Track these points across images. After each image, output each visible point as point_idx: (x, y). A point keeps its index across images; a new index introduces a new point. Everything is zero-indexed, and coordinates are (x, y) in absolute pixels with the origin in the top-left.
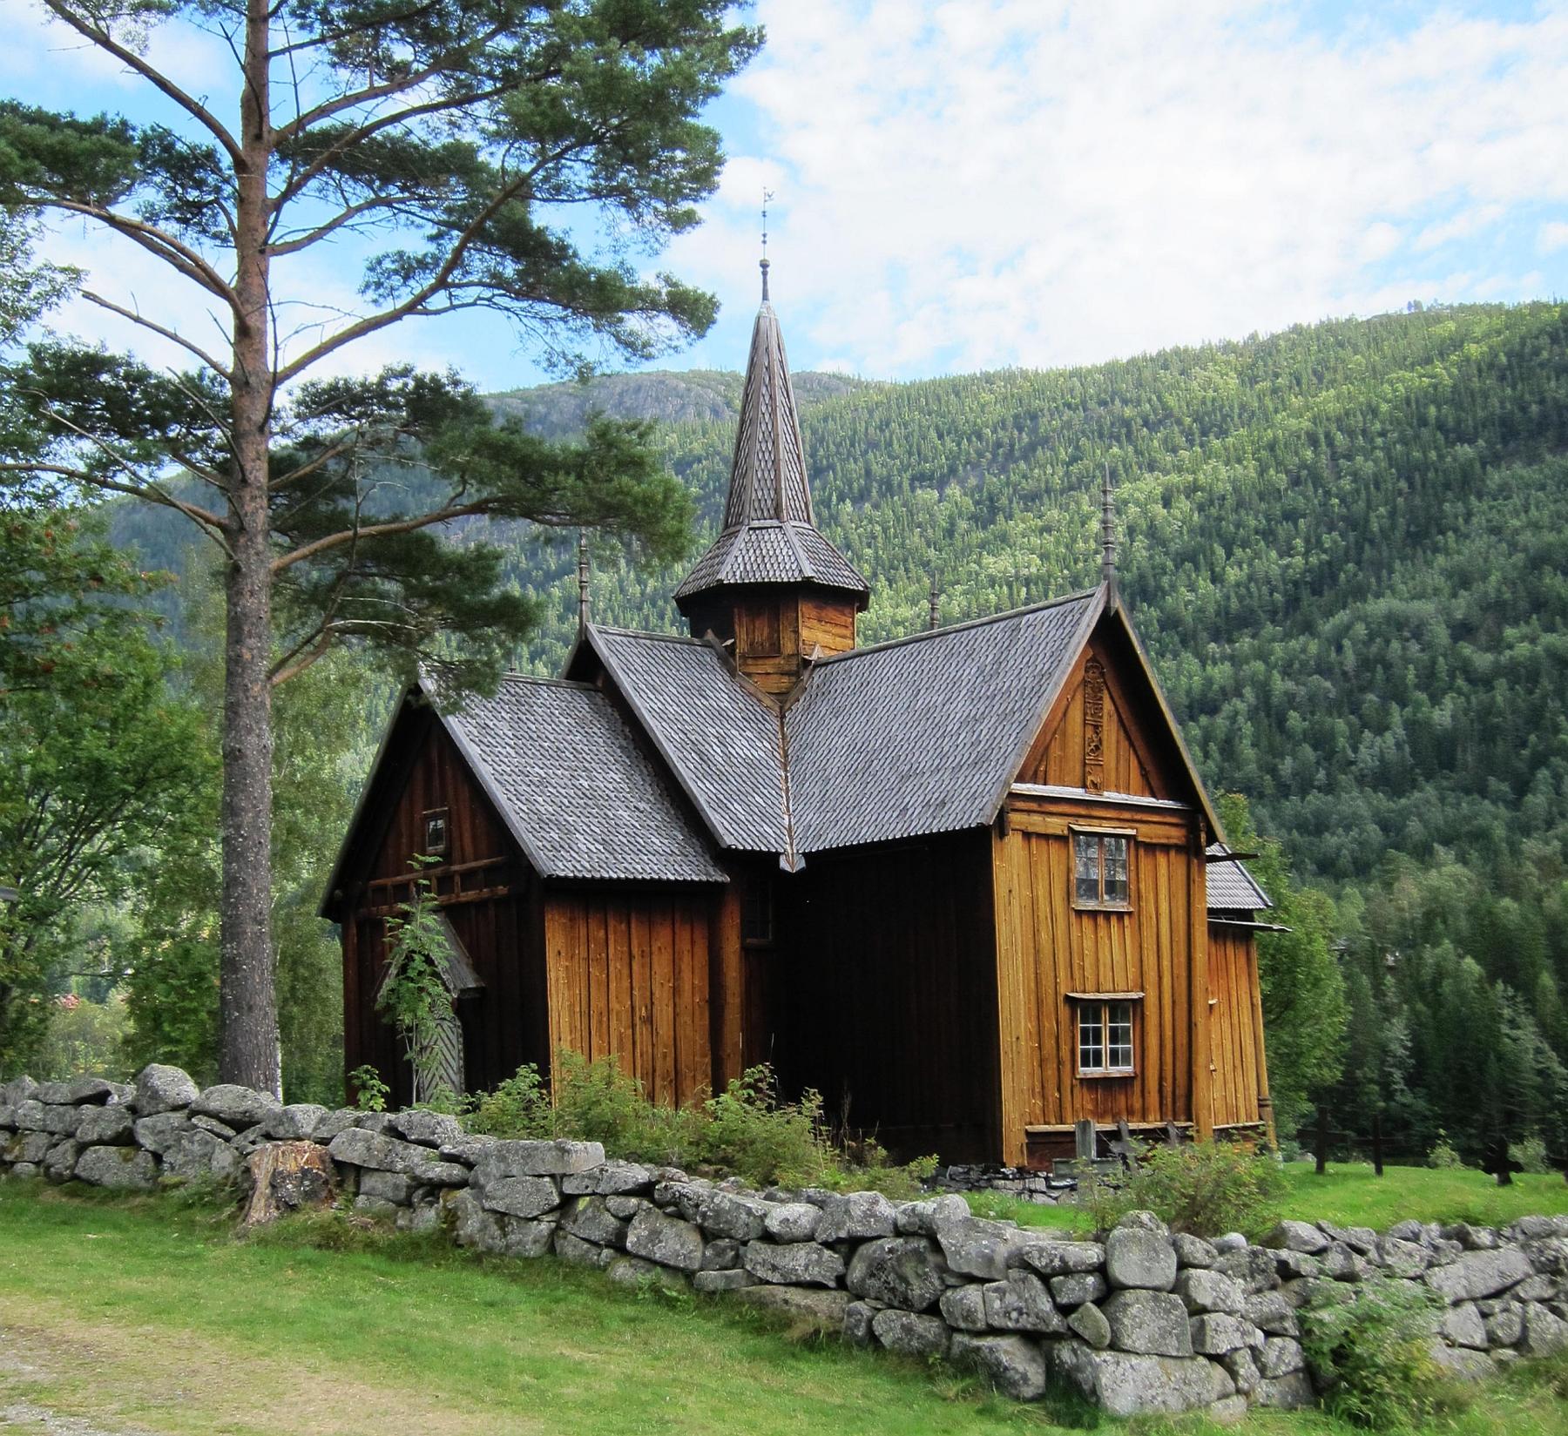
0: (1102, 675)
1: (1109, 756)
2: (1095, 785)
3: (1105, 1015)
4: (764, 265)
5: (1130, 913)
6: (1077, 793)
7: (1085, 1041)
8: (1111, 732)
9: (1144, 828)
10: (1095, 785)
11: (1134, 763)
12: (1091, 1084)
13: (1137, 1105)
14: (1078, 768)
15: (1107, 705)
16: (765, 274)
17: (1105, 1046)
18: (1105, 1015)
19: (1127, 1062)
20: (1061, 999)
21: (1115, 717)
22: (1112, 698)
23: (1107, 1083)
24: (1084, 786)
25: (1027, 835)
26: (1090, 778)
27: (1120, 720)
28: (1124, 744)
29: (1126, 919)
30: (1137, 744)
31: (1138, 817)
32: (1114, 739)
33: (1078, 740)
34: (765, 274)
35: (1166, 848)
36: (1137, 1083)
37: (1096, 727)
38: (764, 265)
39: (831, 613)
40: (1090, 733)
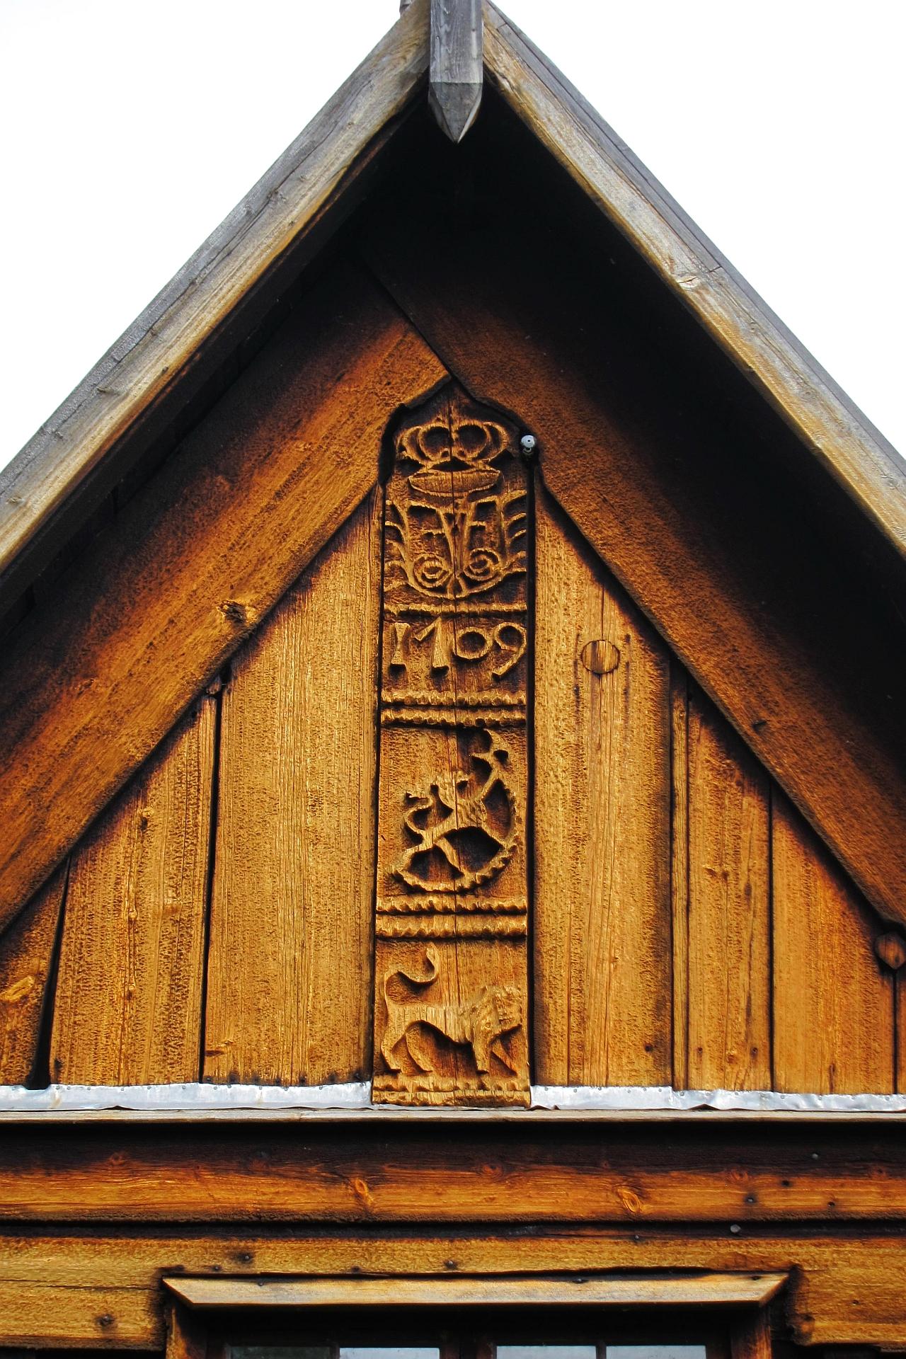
0: (528, 465)
1: (593, 884)
2: (455, 1053)
6: (346, 1100)
8: (597, 740)
10: (455, 1053)
11: (806, 906)
14: (332, 966)
15: (571, 611)
21: (643, 674)
22: (605, 576)
24: (370, 1067)
26: (401, 1015)
27: (679, 682)
28: (721, 817)
30: (816, 800)
31: (808, 1196)
32: (623, 780)
33: (342, 821)
37: (471, 737)
40: (429, 768)
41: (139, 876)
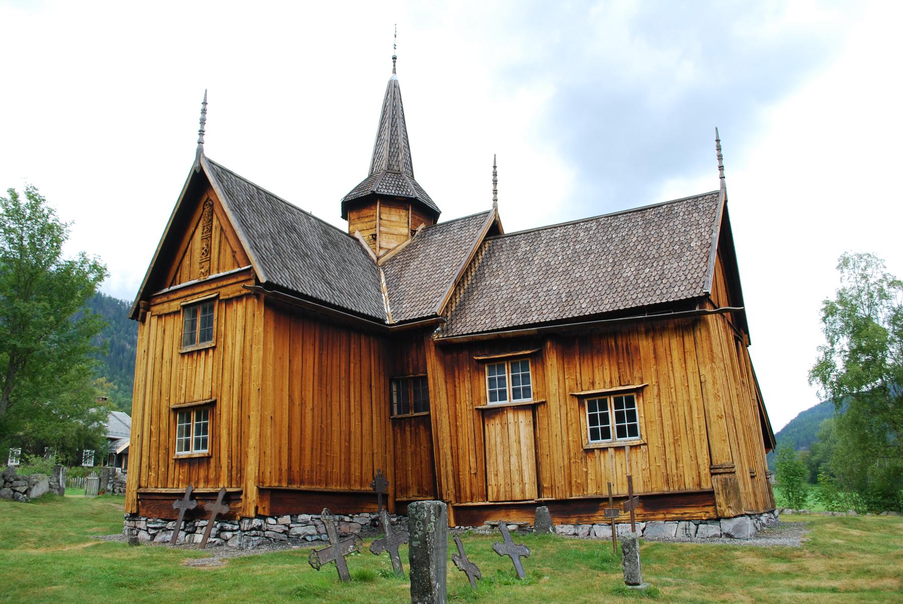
3: (194, 416)
4: (394, 58)
5: (214, 348)
7: (181, 435)
9: (223, 291)
12: (181, 462)
13: (212, 476)
16: (394, 62)
17: (193, 437)
18: (194, 416)
19: (205, 447)
20: (164, 411)
23: (190, 461)
25: (160, 316)
29: (211, 352)
31: (220, 284)
34: (394, 62)
35: (239, 298)
36: (212, 461)
38: (394, 58)
39: (366, 212)
41: (186, 261)
